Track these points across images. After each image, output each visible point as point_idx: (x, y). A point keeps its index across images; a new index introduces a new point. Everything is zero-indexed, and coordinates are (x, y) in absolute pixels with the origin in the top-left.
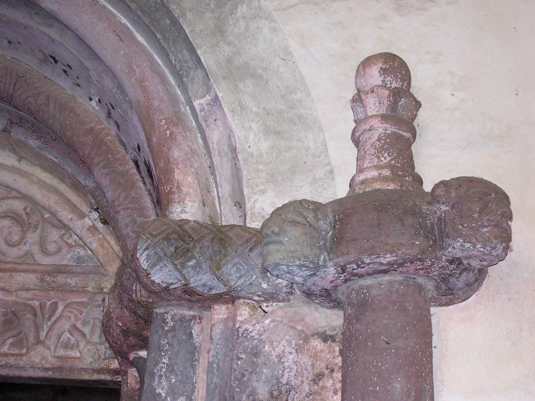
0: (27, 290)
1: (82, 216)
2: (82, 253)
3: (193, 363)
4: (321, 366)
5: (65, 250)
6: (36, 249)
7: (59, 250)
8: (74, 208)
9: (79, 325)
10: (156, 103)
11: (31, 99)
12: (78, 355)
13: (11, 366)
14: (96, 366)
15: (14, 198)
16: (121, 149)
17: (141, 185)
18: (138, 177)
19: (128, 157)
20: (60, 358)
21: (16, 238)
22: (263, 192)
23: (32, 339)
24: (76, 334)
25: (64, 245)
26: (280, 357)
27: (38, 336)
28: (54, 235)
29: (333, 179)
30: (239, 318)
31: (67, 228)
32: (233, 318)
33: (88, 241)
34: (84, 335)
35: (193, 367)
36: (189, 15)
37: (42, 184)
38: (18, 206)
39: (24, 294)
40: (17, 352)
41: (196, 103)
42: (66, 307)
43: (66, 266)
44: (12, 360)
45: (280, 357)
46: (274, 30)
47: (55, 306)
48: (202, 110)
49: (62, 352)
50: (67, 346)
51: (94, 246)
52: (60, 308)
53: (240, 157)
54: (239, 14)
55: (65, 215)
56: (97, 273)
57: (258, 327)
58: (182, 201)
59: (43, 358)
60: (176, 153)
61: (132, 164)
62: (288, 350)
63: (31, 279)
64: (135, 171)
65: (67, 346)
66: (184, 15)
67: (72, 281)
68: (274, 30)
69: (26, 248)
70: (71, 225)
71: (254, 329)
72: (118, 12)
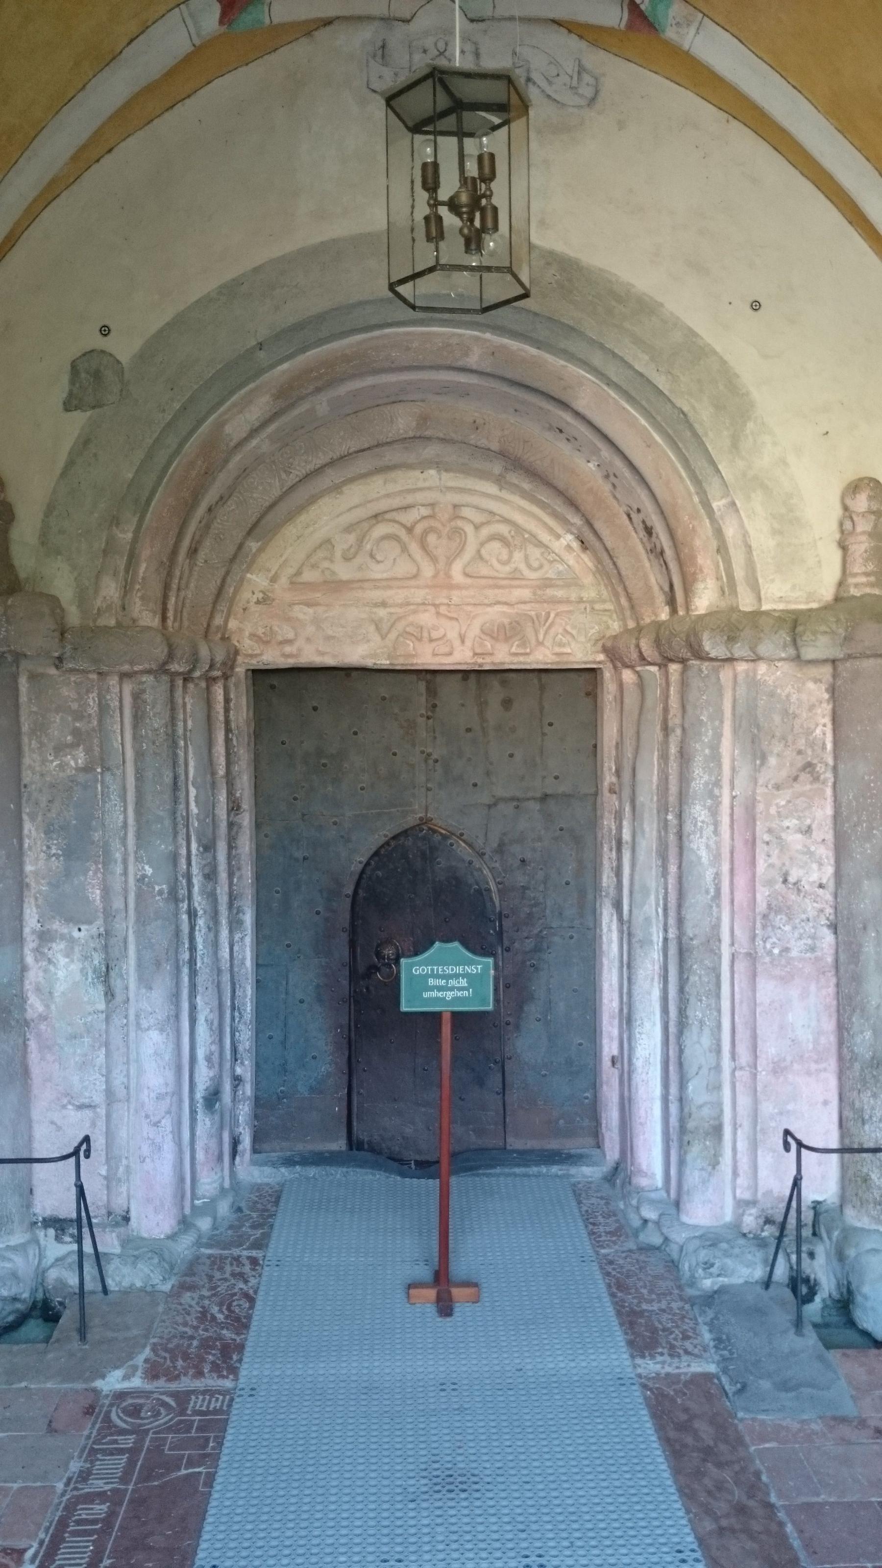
0: (525, 603)
1: (558, 537)
2: (561, 568)
3: (721, 695)
4: (813, 700)
5: (547, 566)
6: (522, 566)
7: (541, 567)
8: (551, 530)
9: (569, 628)
10: (680, 501)
11: (538, 462)
12: (569, 651)
13: (521, 663)
14: (585, 659)
15: (498, 521)
16: (615, 503)
17: (633, 533)
18: (630, 528)
19: (621, 510)
20: (557, 654)
21: (505, 557)
22: (773, 581)
23: (533, 642)
24: (568, 637)
25: (545, 562)
26: (788, 696)
27: (537, 640)
28: (535, 553)
29: (820, 567)
30: (760, 672)
31: (547, 547)
32: (755, 671)
33: (565, 558)
34: (573, 637)
35: (722, 700)
36: (710, 434)
37: (523, 510)
38: (503, 529)
39: (523, 606)
40: (522, 651)
41: (715, 505)
42: (557, 615)
43: (551, 579)
44: (521, 659)
45: (788, 696)
46: (775, 444)
47: (548, 614)
48: (720, 510)
49: (557, 650)
50: (561, 645)
51: (571, 562)
52: (552, 615)
53: (754, 553)
54: (748, 432)
55: (545, 537)
56: (576, 585)
57: (773, 677)
58: (704, 580)
59: (545, 656)
60: (698, 543)
61: (625, 517)
62: (792, 691)
63: (526, 594)
64: (627, 522)
65: (561, 645)
66: (706, 434)
67: (560, 593)
68: (775, 444)
69: (513, 566)
70: (550, 545)
71: (770, 680)
72: (640, 414)
